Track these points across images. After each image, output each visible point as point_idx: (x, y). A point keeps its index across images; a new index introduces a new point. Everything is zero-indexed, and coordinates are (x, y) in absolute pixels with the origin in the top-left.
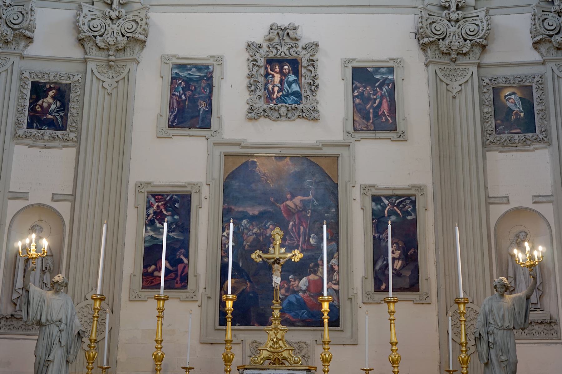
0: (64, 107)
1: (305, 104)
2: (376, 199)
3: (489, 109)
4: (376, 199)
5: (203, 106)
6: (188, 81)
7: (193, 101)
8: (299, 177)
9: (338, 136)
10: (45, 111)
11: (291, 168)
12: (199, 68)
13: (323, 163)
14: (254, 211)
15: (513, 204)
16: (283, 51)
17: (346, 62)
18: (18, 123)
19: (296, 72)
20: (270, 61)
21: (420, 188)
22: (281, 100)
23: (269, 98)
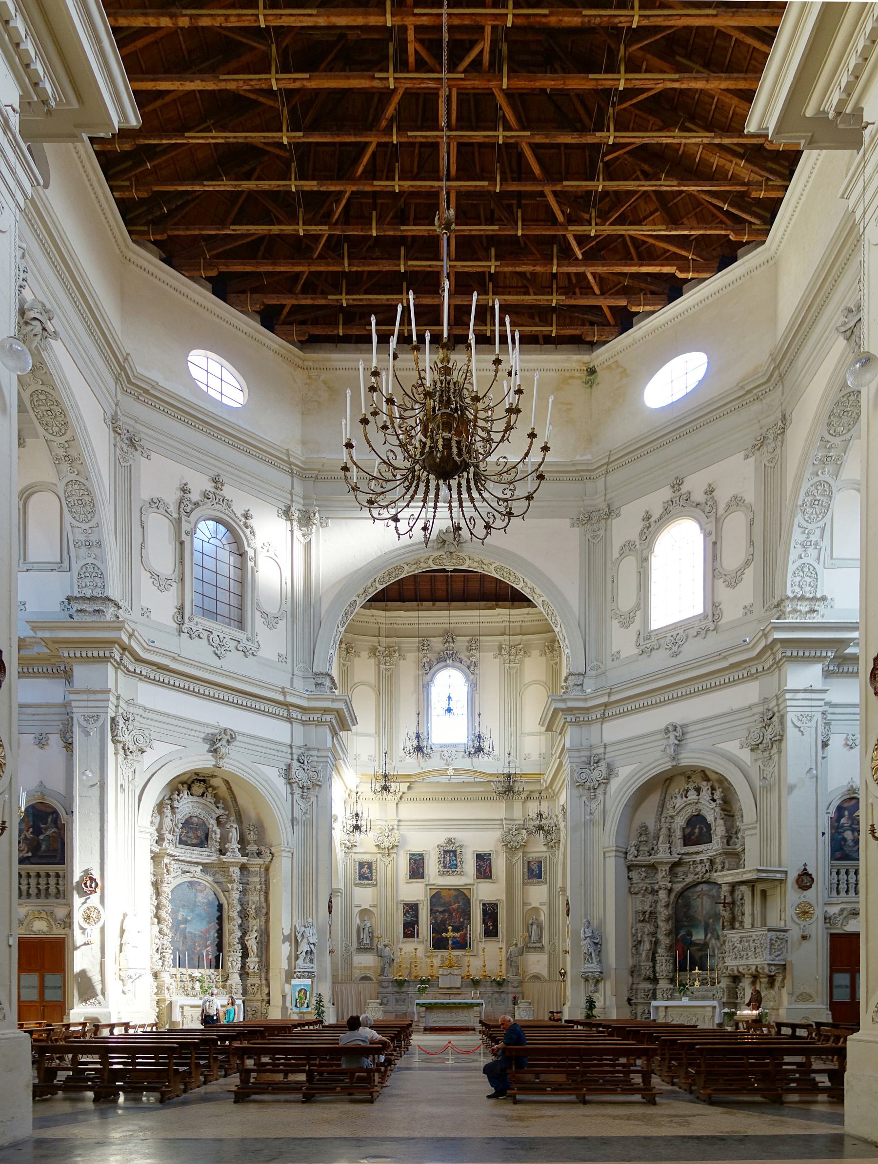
0: (371, 871)
1: (458, 869)
2: (484, 905)
3: (526, 870)
4: (484, 905)
5: (421, 870)
6: (415, 860)
7: (417, 868)
8: (456, 897)
9: (470, 881)
10: (364, 873)
11: (454, 893)
12: (419, 855)
13: (465, 891)
14: (441, 909)
15: (533, 906)
16: (450, 848)
17: (474, 851)
18: (355, 879)
19: (456, 856)
20: (445, 852)
21: (499, 900)
22: (449, 867)
23: (445, 867)
